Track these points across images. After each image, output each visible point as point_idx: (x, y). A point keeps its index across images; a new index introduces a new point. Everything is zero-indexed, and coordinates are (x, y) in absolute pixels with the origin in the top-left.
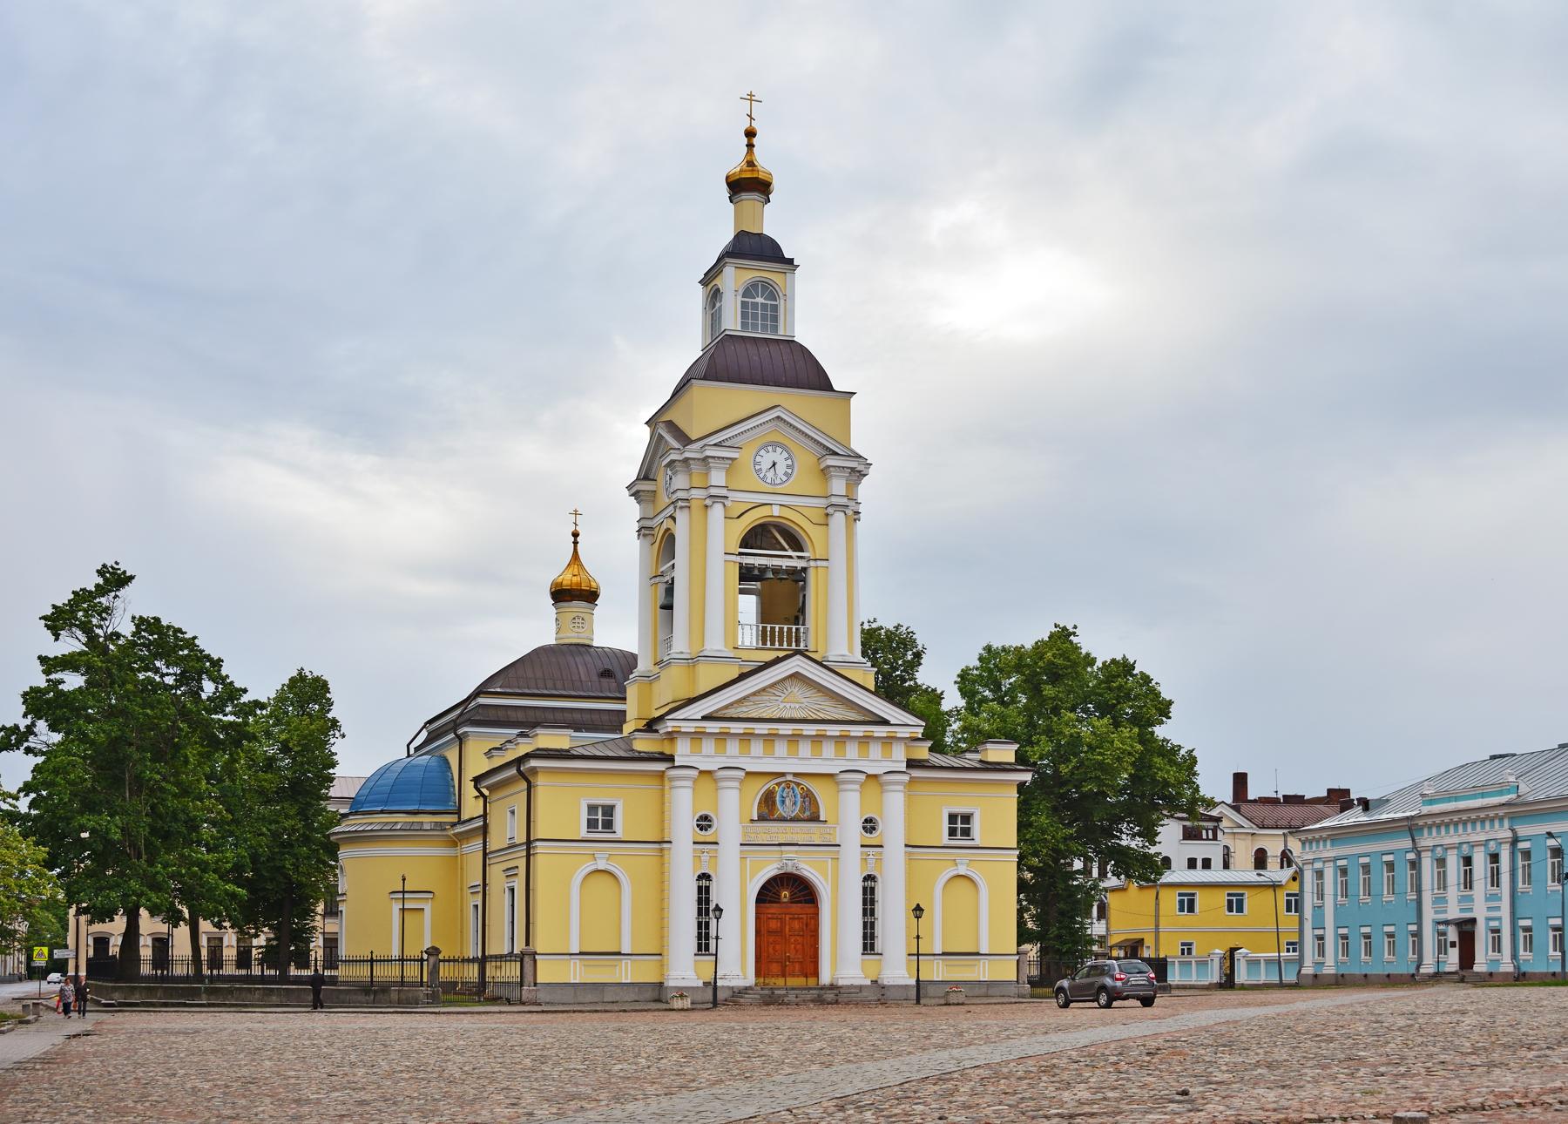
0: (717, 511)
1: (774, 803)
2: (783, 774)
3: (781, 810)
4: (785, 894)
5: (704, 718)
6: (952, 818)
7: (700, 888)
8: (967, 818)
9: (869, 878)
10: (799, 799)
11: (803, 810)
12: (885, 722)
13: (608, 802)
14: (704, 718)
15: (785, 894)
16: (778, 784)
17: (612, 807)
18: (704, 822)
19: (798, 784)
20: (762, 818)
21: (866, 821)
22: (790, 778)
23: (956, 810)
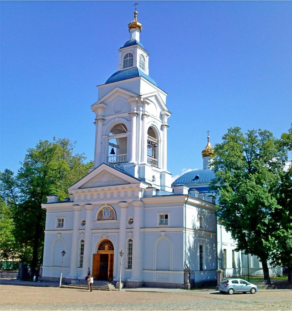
0: (100, 123)
1: (102, 215)
2: (104, 205)
3: (104, 217)
4: (106, 246)
5: (80, 188)
6: (161, 217)
7: (82, 245)
8: (166, 217)
9: (130, 240)
10: (109, 213)
11: (110, 216)
12: (130, 183)
13: (61, 218)
14: (80, 188)
15: (106, 246)
16: (104, 208)
17: (63, 220)
18: (84, 223)
19: (109, 208)
20: (98, 220)
21: (131, 219)
22: (106, 206)
23: (162, 214)
